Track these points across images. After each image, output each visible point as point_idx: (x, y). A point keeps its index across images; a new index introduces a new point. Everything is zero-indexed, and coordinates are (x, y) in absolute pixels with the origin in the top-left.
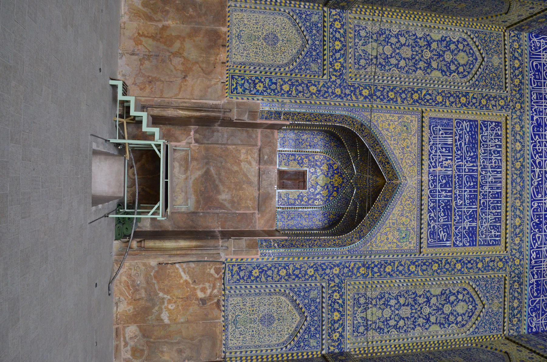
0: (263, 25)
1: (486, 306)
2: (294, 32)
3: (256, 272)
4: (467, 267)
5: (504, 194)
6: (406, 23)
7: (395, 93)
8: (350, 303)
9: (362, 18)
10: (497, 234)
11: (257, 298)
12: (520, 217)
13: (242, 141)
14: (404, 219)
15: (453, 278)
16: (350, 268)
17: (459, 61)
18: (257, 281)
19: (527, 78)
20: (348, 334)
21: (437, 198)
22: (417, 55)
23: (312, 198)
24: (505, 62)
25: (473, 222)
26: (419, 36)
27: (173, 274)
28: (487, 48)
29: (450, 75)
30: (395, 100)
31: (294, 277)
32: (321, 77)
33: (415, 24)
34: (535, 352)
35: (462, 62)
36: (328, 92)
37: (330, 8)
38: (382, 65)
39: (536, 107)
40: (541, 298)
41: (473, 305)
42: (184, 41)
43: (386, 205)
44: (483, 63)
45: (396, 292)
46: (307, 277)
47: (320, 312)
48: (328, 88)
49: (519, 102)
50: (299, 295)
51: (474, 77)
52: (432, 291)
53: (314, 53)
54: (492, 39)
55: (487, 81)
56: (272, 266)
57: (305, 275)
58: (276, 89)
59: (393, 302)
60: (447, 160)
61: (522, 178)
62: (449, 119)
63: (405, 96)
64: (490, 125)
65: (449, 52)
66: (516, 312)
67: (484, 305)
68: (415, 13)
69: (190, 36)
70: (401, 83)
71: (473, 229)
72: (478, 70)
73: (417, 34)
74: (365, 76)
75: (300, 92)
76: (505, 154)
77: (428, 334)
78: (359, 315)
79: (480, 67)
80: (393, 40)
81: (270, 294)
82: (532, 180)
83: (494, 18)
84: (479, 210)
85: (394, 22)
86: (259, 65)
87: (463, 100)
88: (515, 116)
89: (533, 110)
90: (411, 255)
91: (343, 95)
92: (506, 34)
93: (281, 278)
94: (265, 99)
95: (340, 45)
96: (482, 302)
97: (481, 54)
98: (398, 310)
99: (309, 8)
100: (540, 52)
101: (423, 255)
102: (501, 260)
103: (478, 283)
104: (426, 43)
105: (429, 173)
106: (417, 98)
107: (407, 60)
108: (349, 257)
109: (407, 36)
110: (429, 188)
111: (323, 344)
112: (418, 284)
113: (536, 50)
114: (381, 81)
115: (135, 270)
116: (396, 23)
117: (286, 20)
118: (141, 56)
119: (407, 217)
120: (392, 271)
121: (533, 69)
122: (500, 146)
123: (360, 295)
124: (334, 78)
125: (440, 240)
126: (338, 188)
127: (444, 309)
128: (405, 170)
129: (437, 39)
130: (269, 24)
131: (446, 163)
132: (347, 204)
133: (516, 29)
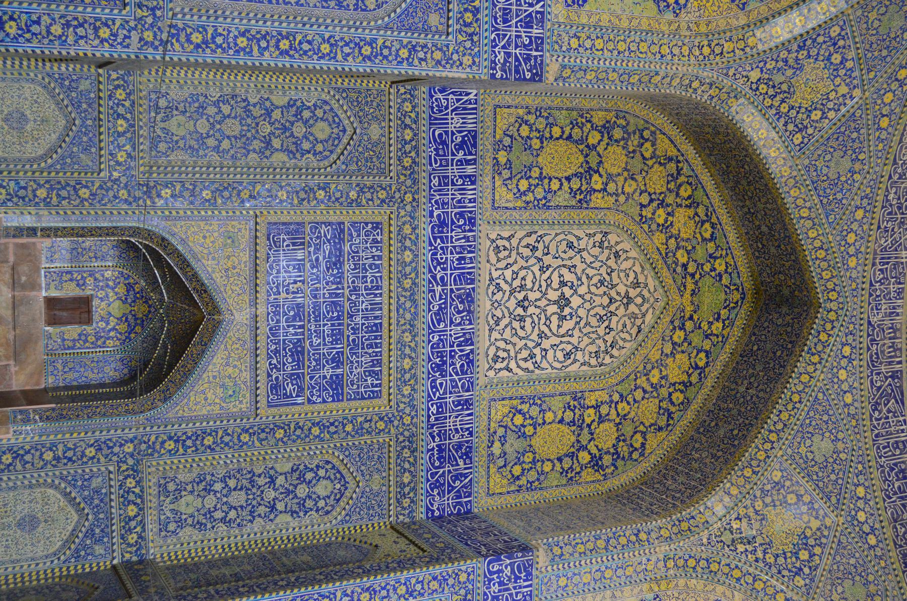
1: (360, 484)
2: (53, 106)
5: (385, 325)
8: (154, 491)
12: (410, 357)
14: (230, 370)
15: (307, 448)
16: (150, 443)
17: (317, 136)
19: (424, 155)
20: (151, 534)
21: (282, 338)
22: (249, 131)
23: (102, 337)
28: (361, 114)
29: (302, 156)
32: (95, 174)
34: (414, 543)
35: (321, 136)
39: (438, 197)
40: (447, 469)
41: (342, 483)
43: (203, 352)
44: (354, 137)
45: (222, 472)
46: (85, 460)
47: (108, 506)
48: (107, 191)
50: (74, 485)
51: (339, 158)
53: (85, 139)
54: (369, 99)
55: (360, 163)
56: (32, 447)
57: (82, 457)
60: (295, 282)
61: (414, 301)
62: (298, 224)
64: (364, 228)
65: (300, 123)
66: (407, 490)
72: (346, 148)
73: (250, 99)
76: (387, 268)
77: (273, 527)
78: (168, 506)
79: (349, 144)
80: (211, 110)
81: (30, 487)
82: (430, 303)
88: (403, 213)
89: (433, 201)
92: (392, 90)
93: (46, 464)
95: (125, 125)
96: (355, 478)
97: (352, 123)
98: (226, 496)
100: (447, 114)
101: (261, 418)
102: (381, 419)
103: (347, 453)
104: (263, 112)
107: (233, 139)
108: (148, 429)
109: (232, 102)
111: (113, 551)
112: (255, 459)
113: (441, 111)
117: (39, 88)
120: (214, 443)
121: (435, 141)
123: (168, 480)
126: (143, 321)
127: (297, 491)
128: (230, 301)
129: (282, 104)
132: (156, 345)
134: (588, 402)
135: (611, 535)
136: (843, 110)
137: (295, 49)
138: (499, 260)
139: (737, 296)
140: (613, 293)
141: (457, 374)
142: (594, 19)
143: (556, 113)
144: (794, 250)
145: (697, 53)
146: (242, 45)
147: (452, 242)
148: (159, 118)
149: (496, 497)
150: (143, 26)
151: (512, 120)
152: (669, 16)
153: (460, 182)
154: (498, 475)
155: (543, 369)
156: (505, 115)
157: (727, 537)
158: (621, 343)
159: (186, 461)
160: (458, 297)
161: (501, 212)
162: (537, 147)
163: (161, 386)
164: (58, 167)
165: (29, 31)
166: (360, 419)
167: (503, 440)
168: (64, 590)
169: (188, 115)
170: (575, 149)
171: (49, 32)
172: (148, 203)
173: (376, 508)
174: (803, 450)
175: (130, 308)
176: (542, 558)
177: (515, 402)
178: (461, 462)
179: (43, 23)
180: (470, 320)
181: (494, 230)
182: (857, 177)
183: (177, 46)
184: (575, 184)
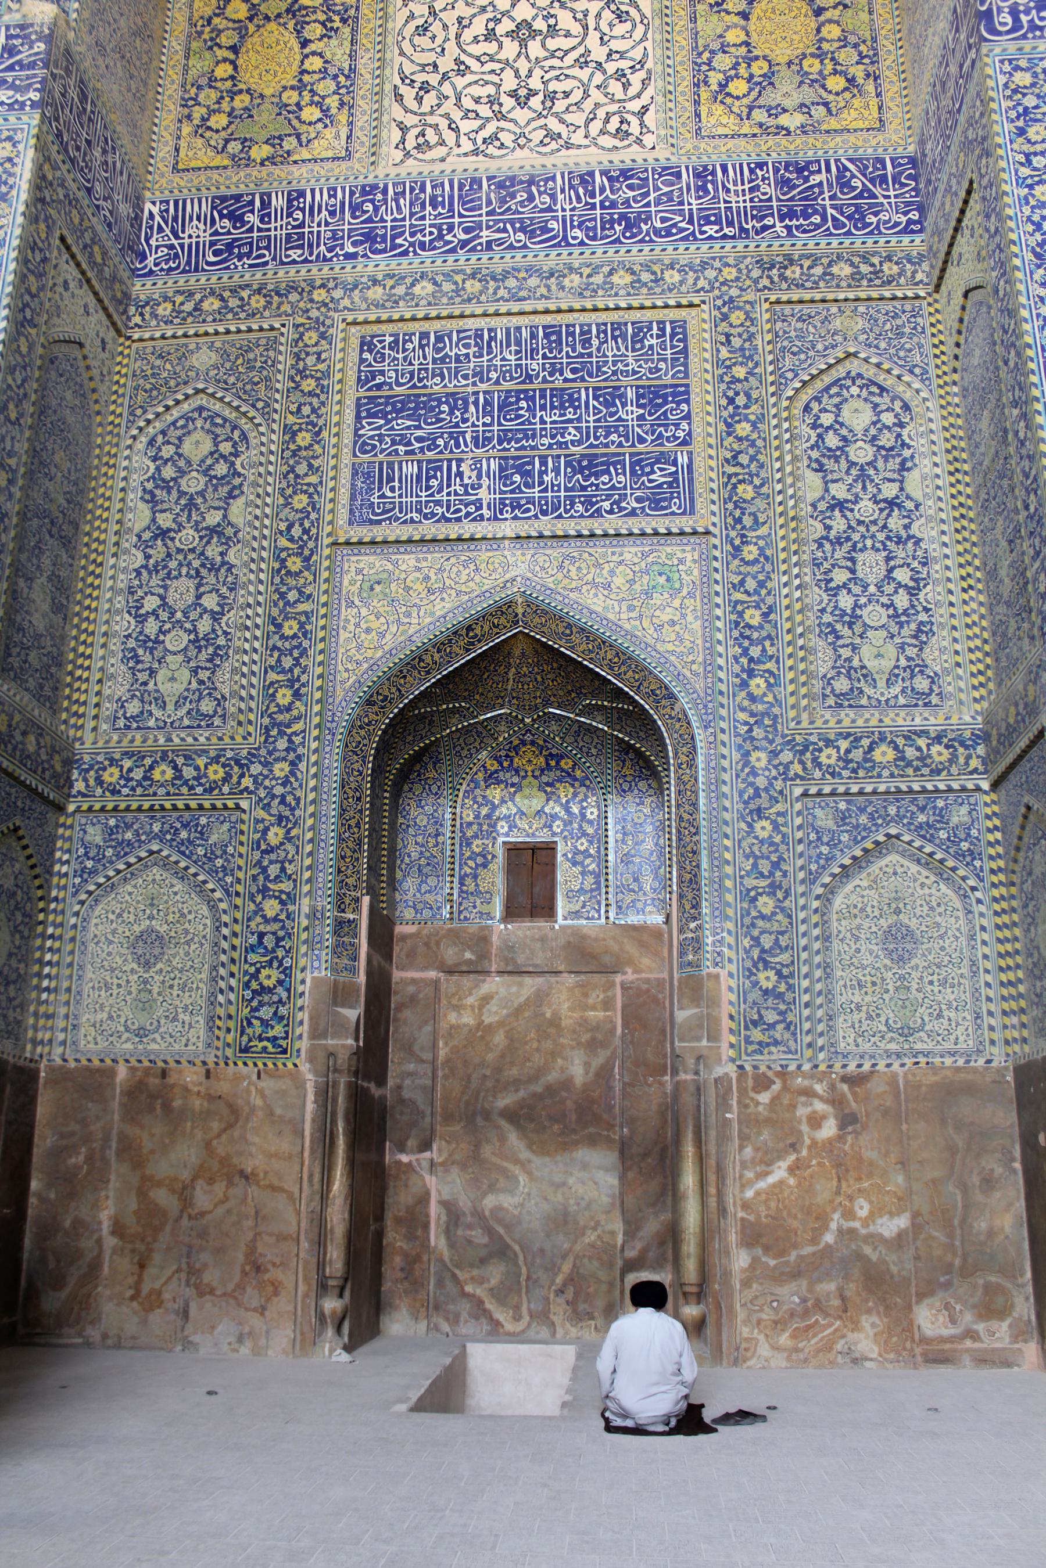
0: (113, 970)
1: (852, 350)
2: (129, 888)
3: (767, 979)
4: (746, 407)
5: (548, 319)
6: (108, 595)
7: (286, 618)
8: (847, 716)
9: (94, 712)
10: (655, 331)
11: (839, 973)
12: (610, 274)
13: (426, 1023)
14: (618, 581)
16: (752, 721)
18: (791, 975)
19: (247, 276)
20: (933, 721)
22: (189, 564)
24: (206, 334)
25: (623, 396)
26: (140, 560)
27: (773, 1204)
28: (172, 383)
29: (239, 475)
30: (303, 619)
31: (778, 874)
32: (245, 817)
33: (111, 573)
34: (959, 221)
35: (207, 446)
36: (283, 797)
37: (69, 796)
38: (215, 654)
39: (322, 248)
40: (827, 202)
41: (849, 383)
42: (151, 1178)
43: (583, 630)
44: (210, 391)
45: (817, 595)
46: (778, 839)
47: (873, 798)
48: (274, 797)
49: (310, 293)
50: (827, 860)
52: (812, 496)
58: (274, 933)
59: (846, 601)
60: (460, 474)
61: (506, 275)
62: (355, 473)
63: (294, 592)
65: (183, 482)
66: (865, 269)
67: (849, 355)
68: (82, 574)
69: (138, 1164)
70: (259, 604)
71: (643, 396)
72: (229, 404)
73: (137, 565)
74: (242, 699)
75: (283, 869)
78: (881, 691)
79: (221, 399)
80: (151, 627)
82: (511, 247)
83: (95, 372)
84: (593, 382)
85: (104, 628)
86: (214, 980)
87: (304, 439)
88: (346, 302)
90: (716, 559)
91: (292, 756)
92: (136, 336)
93: (782, 909)
94: (302, 962)
95: (163, 767)
96: (839, 361)
97: (187, 397)
98: (865, 587)
99: (69, 851)
100: (182, 246)
102: (725, 317)
103: (790, 375)
104: (159, 542)
105: (496, 519)
106: (298, 560)
109: (140, 593)
110: (536, 516)
111: (964, 789)
112: (794, 536)
113: (176, 256)
114: (256, 657)
115: (761, 1310)
116: (107, 622)
117: (99, 910)
118: (189, 1292)
119: (612, 572)
120: (757, 607)
122: (424, 335)
123: (828, 691)
124: (247, 782)
127: (862, 461)
128: (488, 584)
129: (148, 513)
130: (109, 954)
131: (469, 476)
132: (590, 730)
133: (125, 312)
138: (442, 143)
141: (647, 194)
143: (193, 73)
147: (404, 219)
148: (158, 713)
149: (888, 116)
151: (199, 142)
154: (845, 115)
155: (645, 55)
156: (191, 154)
159: (790, 656)
160: (503, 201)
162: (246, 98)
166: (724, 353)
169: (156, 665)
170: (256, 39)
172: (297, 727)
173: (899, 322)
175: (530, 779)
177: (704, 95)
178: (815, 179)
180: (546, 180)
181: (388, 155)
184: (313, 31)
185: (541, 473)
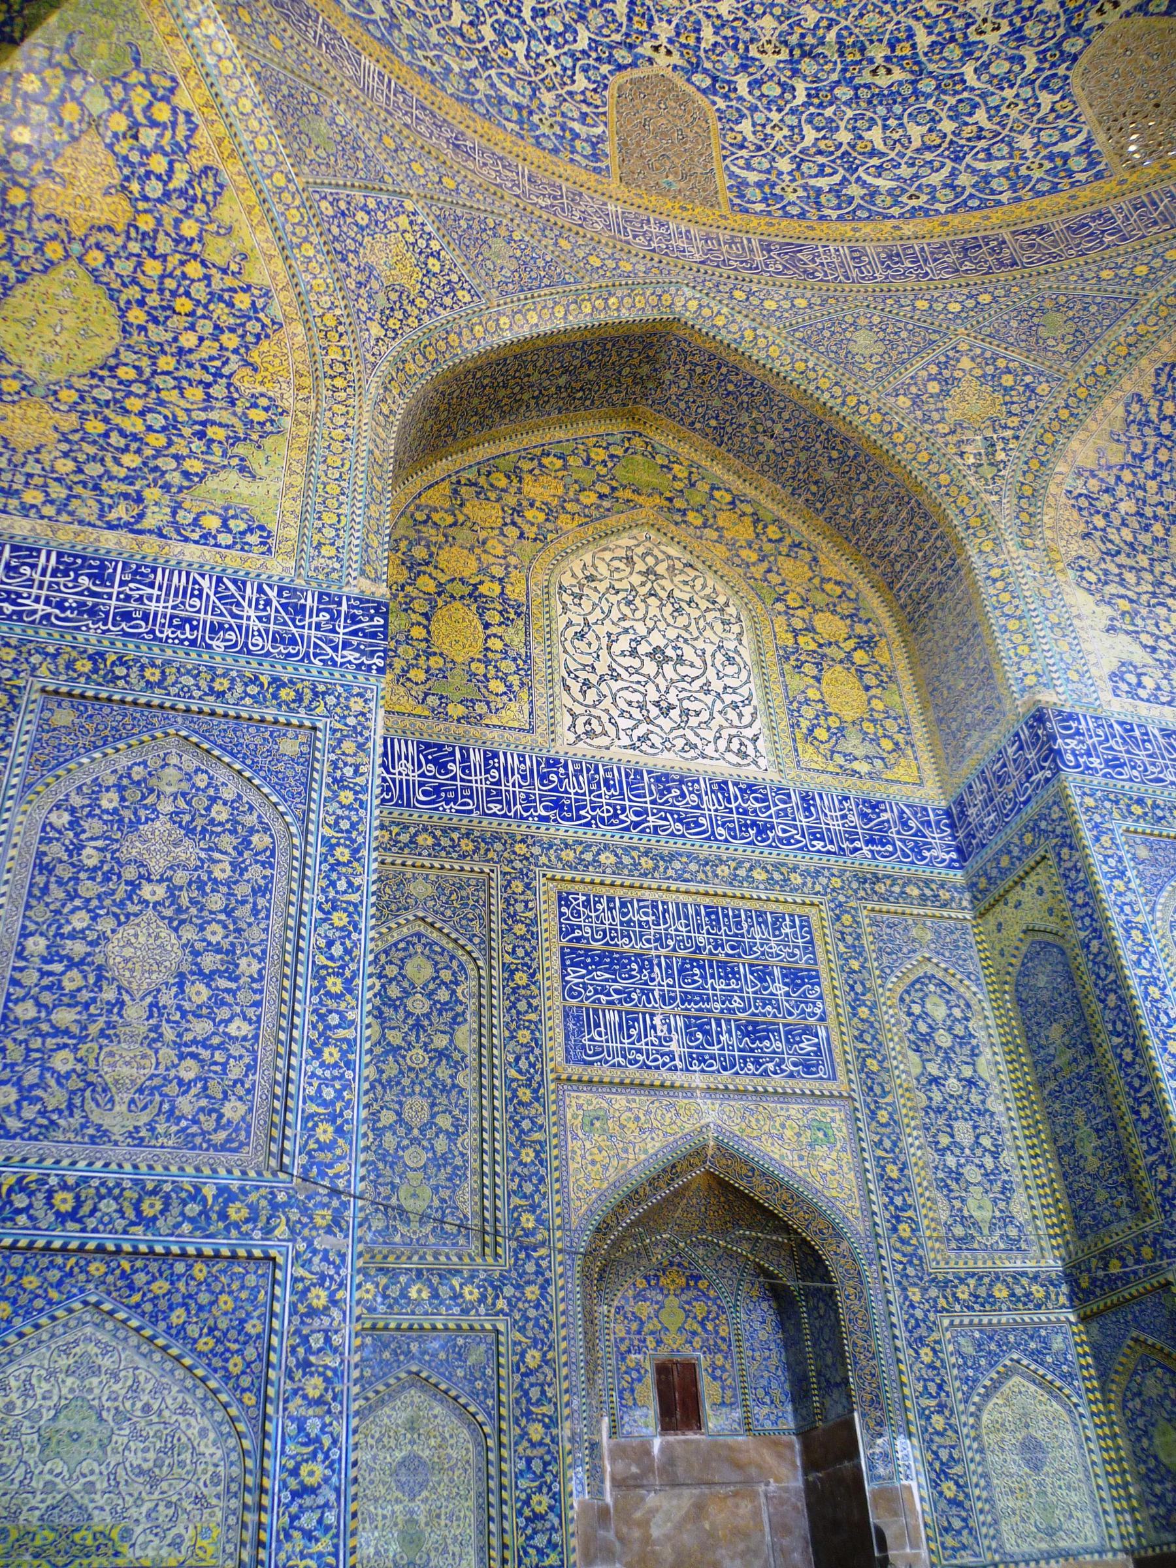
0: (376, 1500)
2: (386, 1410)
5: (707, 901)
12: (751, 869)
14: (788, 1133)
25: (771, 974)
35: (428, 972)
45: (932, 1155)
46: (938, 1364)
48: (528, 1319)
52: (916, 1071)
60: (653, 1027)
61: (672, 857)
62: (566, 1016)
65: (409, 1002)
66: (928, 892)
79: (440, 930)
80: (389, 1141)
87: (521, 978)
102: (838, 918)
119: (783, 1126)
122: (611, 899)
125: (818, 1053)
128: (688, 1128)
130: (372, 1482)
131: (662, 1030)
134: (790, 643)
135: (998, 613)
136: (428, 228)
137: (342, 967)
139: (637, 441)
140: (643, 590)
141: (768, 808)
142: (291, 520)
144: (602, 341)
145: (343, 395)
146: (337, 1056)
150: (305, 1225)
152: (286, 422)
153: (494, 772)
157: (988, 472)
158: (708, 591)
161: (536, 722)
163: (815, 1242)
164: (490, 1402)
165: (318, 1440)
166: (842, 949)
167: (850, 757)
168: (1139, 1394)
171: (319, 1402)
172: (543, 1251)
174: (870, 367)
176: (1047, 697)
177: (799, 736)
178: (885, 816)
179: (302, 1411)
182: (517, 236)
183: (340, 1168)
185: (719, 1033)
